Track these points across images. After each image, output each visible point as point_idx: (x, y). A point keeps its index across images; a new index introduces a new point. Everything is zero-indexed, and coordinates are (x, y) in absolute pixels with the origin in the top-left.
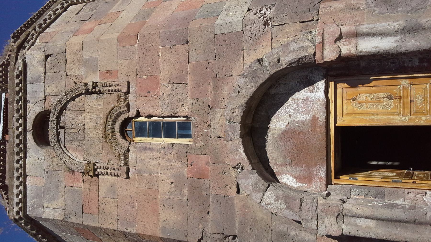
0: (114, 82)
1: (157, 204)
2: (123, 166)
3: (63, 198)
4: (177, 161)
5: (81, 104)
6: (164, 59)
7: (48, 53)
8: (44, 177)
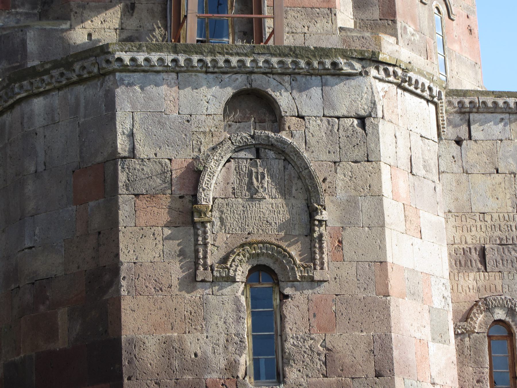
0: (327, 254)
1: (165, 331)
2: (213, 276)
3: (152, 156)
4: (226, 362)
5: (294, 191)
6: (357, 340)
7: (367, 122)
8: (179, 113)
